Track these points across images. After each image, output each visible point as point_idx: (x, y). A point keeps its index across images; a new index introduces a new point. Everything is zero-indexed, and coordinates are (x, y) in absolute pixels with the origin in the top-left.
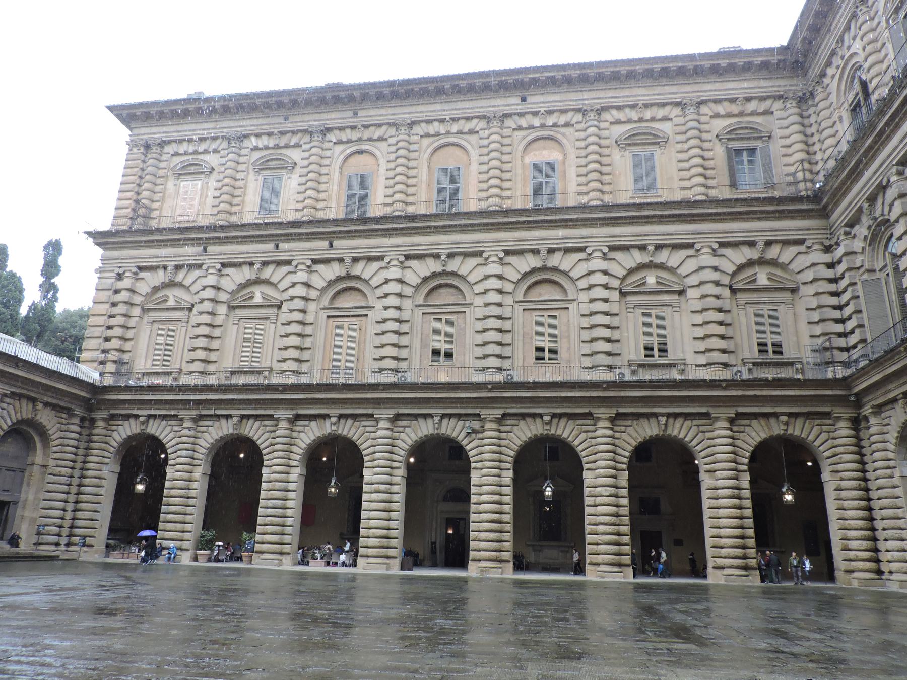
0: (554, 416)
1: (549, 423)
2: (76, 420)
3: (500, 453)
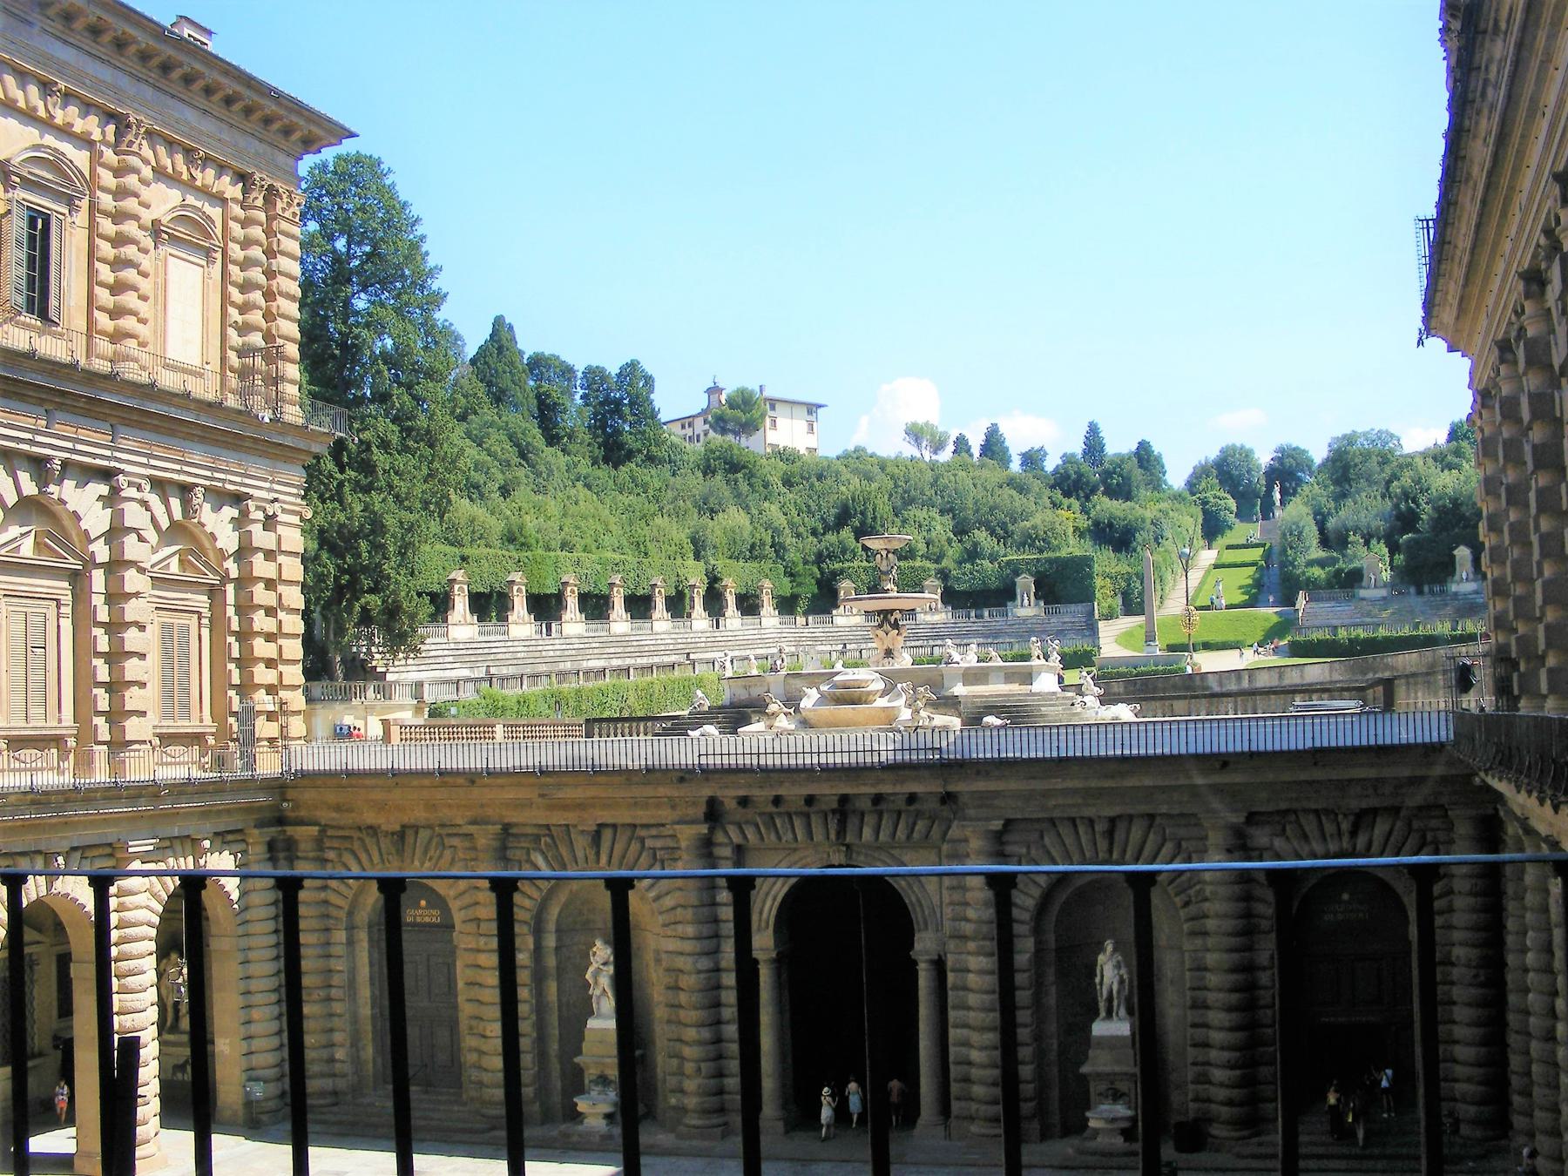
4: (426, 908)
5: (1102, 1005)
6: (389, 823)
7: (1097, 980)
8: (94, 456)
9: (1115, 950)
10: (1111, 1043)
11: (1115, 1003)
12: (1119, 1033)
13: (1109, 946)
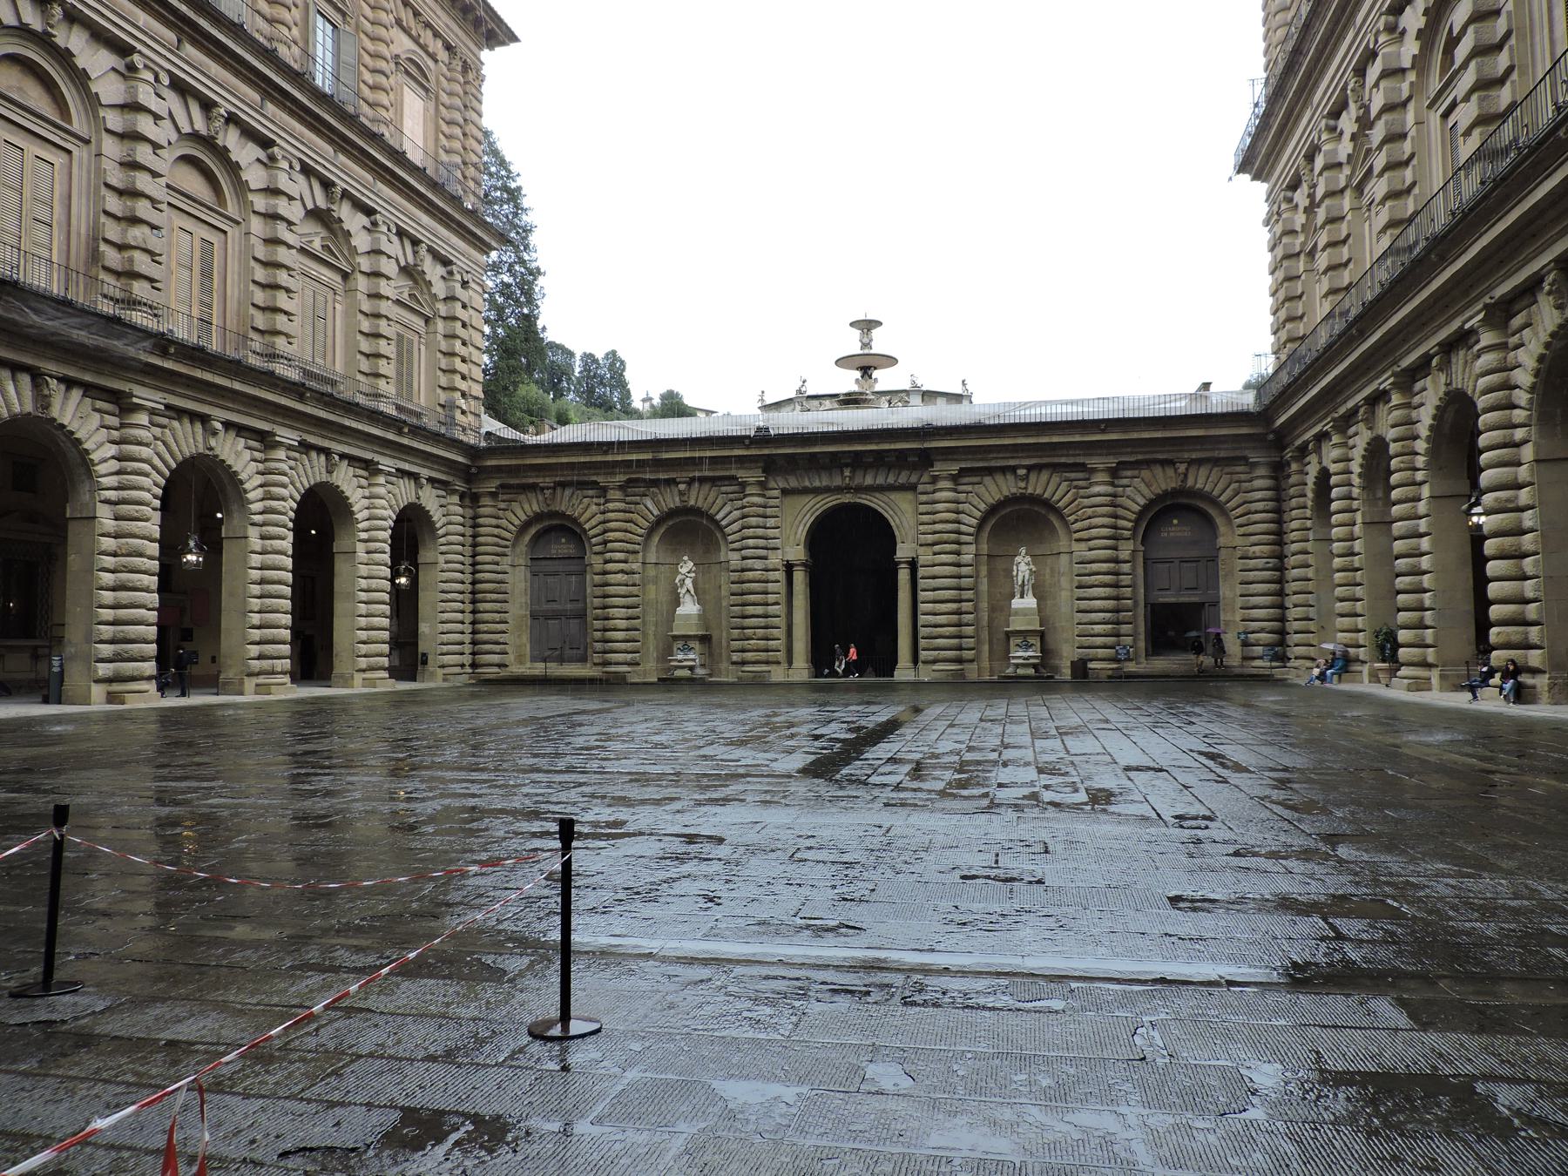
0: (1030, 468)
1: (1026, 478)
2: (456, 499)
3: (959, 523)
5: (1017, 589)
8: (363, 194)
10: (1024, 612)
13: (1023, 550)
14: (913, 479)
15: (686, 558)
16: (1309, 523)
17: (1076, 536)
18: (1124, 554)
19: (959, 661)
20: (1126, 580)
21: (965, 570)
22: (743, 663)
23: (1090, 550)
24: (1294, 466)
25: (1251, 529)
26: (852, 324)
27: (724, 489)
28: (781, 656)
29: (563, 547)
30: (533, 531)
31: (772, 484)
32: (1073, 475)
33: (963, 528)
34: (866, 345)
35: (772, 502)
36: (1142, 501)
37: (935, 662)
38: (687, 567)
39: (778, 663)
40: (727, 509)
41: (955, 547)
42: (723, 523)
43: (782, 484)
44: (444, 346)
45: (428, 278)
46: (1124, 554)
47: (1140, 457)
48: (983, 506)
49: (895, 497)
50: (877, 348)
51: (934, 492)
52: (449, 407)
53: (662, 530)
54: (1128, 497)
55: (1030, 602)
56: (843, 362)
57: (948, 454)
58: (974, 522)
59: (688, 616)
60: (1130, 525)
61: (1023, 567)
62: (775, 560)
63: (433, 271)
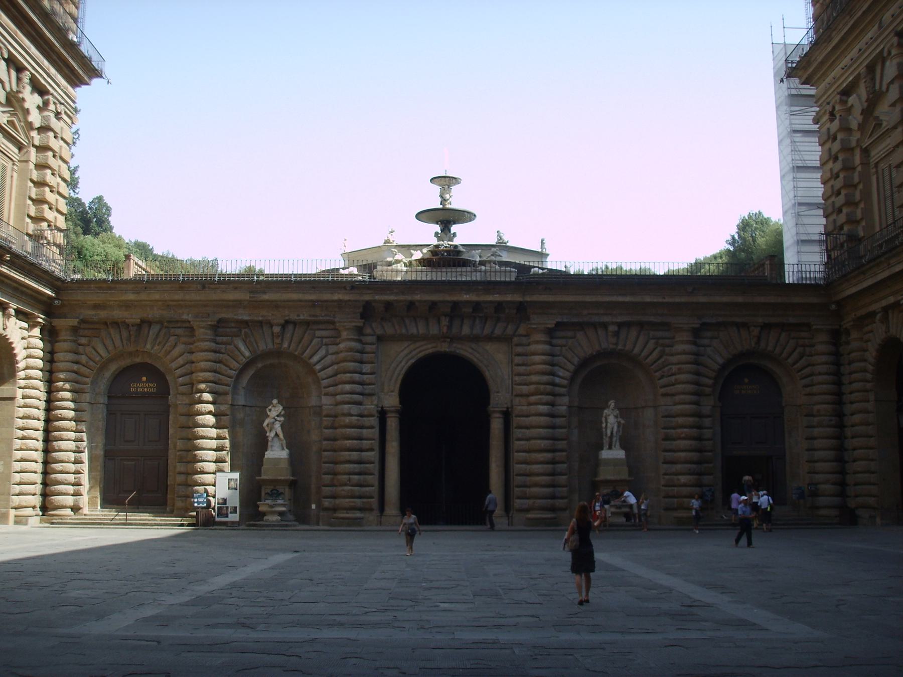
0: (620, 325)
1: (617, 334)
2: (36, 331)
4: (146, 382)
5: (606, 441)
6: (133, 317)
7: (604, 425)
9: (615, 407)
10: (615, 462)
11: (614, 439)
12: (619, 457)
13: (612, 404)
14: (510, 330)
15: (275, 401)
16: (869, 386)
17: (663, 390)
18: (706, 410)
19: (553, 509)
20: (708, 433)
21: (558, 421)
22: (335, 509)
23: (675, 404)
24: (854, 335)
25: (815, 389)
26: (433, 180)
27: (318, 333)
28: (374, 502)
29: (144, 386)
30: (113, 368)
31: (368, 331)
32: (659, 334)
33: (557, 380)
34: (444, 201)
35: (368, 348)
36: (721, 361)
37: (527, 510)
38: (275, 410)
39: (371, 510)
40: (322, 352)
41: (550, 398)
42: (318, 367)
43: (379, 331)
44: (35, 175)
45: (26, 105)
46: (706, 410)
47: (721, 319)
48: (576, 360)
49: (489, 347)
50: (455, 205)
51: (529, 345)
52: (37, 237)
53: (251, 372)
54: (709, 357)
55: (618, 454)
56: (424, 216)
57: (545, 307)
58: (567, 374)
59: (277, 461)
60: (710, 382)
61: (612, 419)
62: (370, 406)
63: (32, 100)
